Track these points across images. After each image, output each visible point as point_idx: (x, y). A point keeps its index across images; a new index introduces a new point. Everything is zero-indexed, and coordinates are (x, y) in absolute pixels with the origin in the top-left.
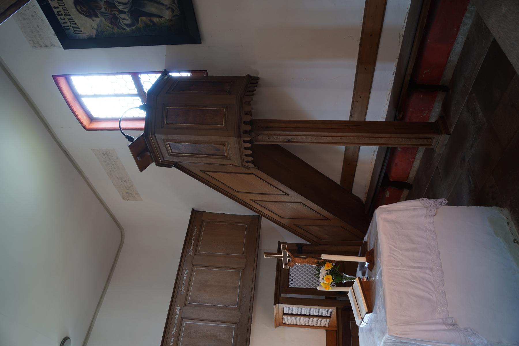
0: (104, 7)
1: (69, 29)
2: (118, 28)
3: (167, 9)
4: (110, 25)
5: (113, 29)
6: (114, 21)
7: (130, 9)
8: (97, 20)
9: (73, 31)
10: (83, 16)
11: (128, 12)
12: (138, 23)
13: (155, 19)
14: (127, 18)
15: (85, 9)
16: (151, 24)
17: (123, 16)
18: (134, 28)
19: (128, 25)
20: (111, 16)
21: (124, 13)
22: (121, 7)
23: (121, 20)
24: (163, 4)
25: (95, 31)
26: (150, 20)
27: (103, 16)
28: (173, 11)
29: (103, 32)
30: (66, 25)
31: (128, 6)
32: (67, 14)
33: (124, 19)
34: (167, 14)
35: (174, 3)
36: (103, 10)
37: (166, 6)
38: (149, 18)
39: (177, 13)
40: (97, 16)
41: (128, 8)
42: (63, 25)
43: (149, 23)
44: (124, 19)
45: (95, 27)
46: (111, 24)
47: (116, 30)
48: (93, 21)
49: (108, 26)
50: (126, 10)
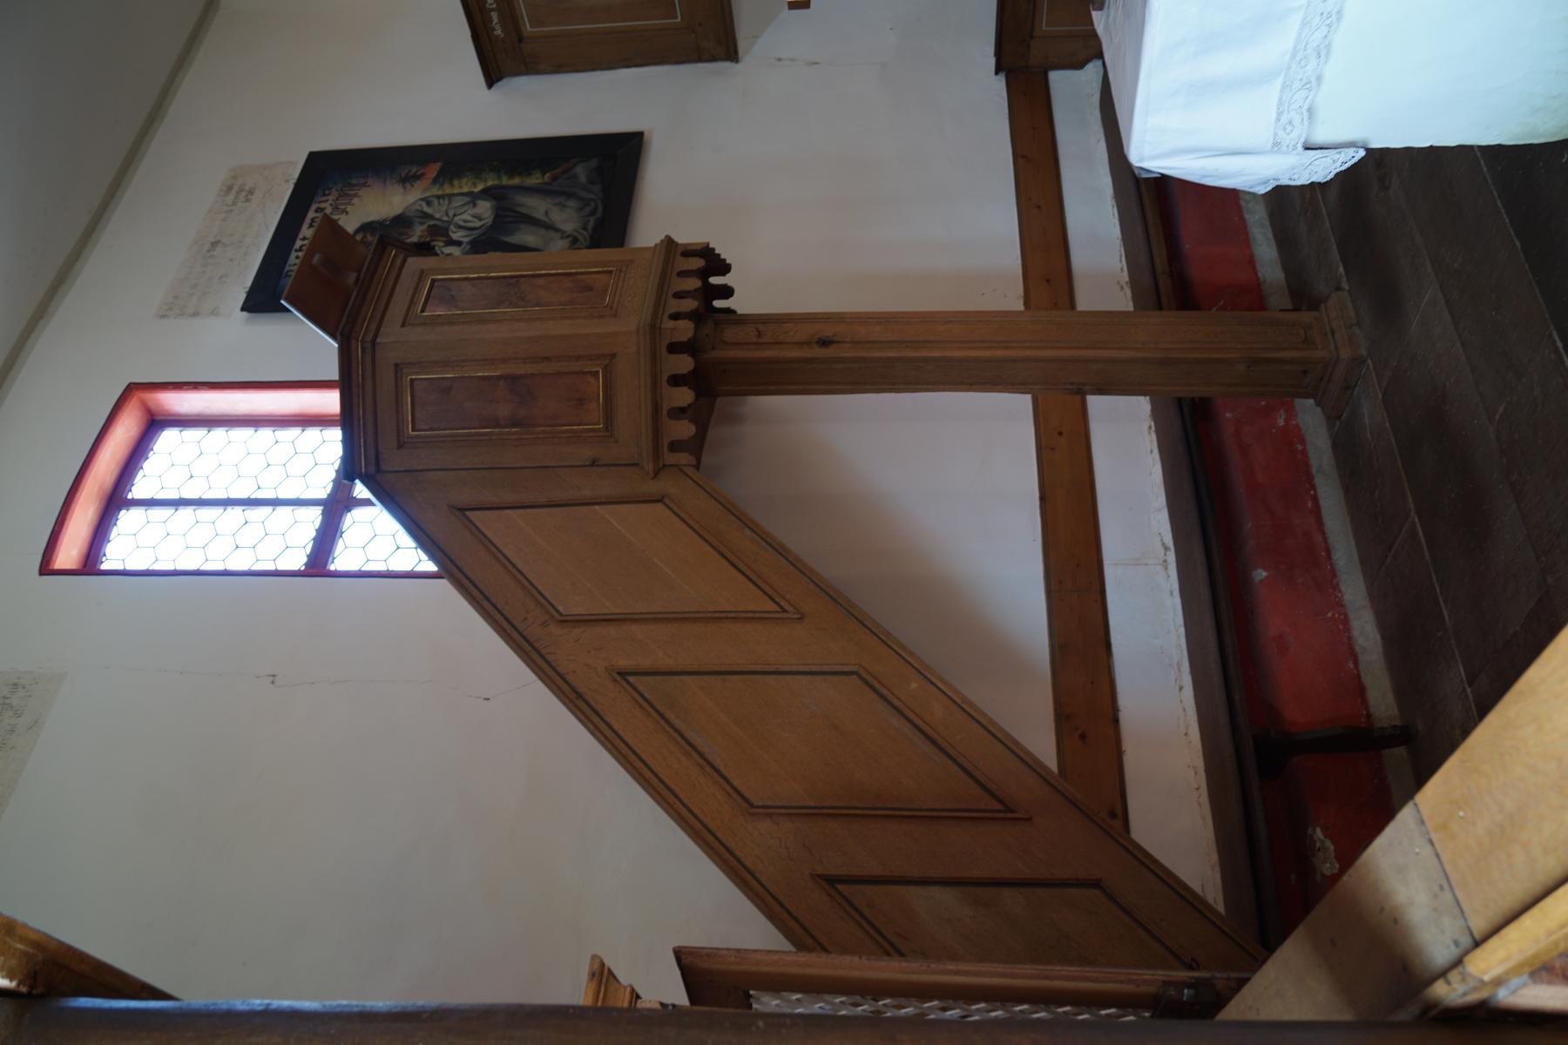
11: (470, 243)
21: (459, 244)
22: (456, 235)
24: (557, 230)
35: (585, 229)
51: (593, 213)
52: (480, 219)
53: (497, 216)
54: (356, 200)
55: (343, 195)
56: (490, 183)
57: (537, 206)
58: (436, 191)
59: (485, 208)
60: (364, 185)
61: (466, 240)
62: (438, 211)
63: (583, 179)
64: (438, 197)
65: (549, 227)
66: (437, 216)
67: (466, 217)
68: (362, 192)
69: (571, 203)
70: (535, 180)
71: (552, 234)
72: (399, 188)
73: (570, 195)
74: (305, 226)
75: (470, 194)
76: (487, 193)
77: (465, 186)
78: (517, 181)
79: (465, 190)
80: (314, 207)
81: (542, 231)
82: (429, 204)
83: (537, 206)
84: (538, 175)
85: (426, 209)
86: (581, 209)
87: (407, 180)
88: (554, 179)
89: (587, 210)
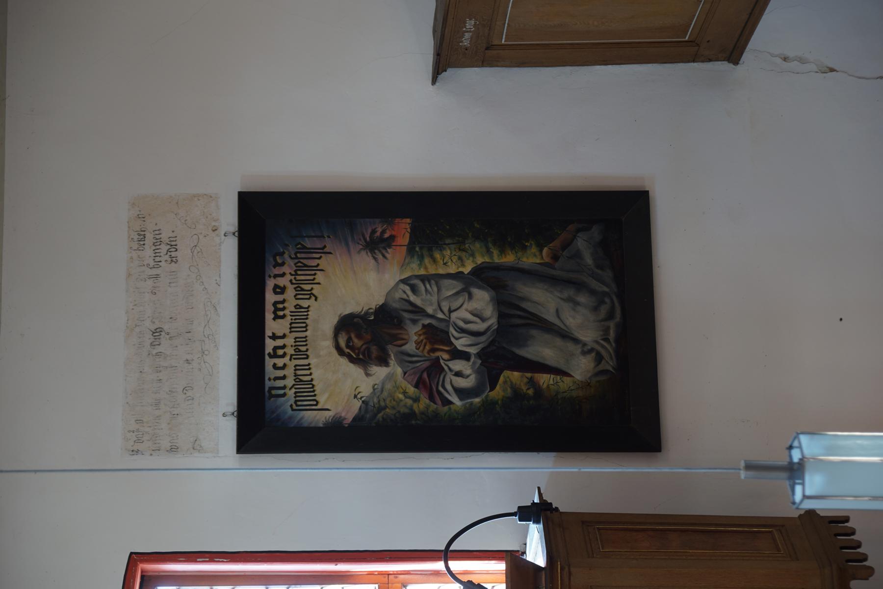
0: (415, 338)
1: (284, 395)
2: (431, 398)
3: (584, 353)
4: (411, 390)
5: (416, 400)
6: (429, 377)
7: (483, 349)
8: (380, 372)
9: (292, 401)
10: (344, 361)
11: (478, 355)
12: (492, 388)
13: (544, 379)
14: (468, 371)
15: (357, 342)
16: (531, 392)
17: (458, 365)
18: (477, 400)
19: (461, 393)
20: (427, 364)
22: (461, 343)
23: (450, 376)
24: (576, 341)
25: (357, 404)
26: (531, 382)
27: (401, 363)
28: (599, 358)
29: (381, 409)
30: (280, 383)
31: (483, 339)
32: (300, 353)
33: (458, 374)
34: (582, 368)
35: (606, 340)
36: (410, 347)
37: (585, 345)
38: (529, 375)
39: (609, 364)
40: (383, 361)
41: (481, 346)
42: (268, 384)
43: (524, 388)
44: (458, 374)
45: (366, 390)
46: (416, 386)
47: (425, 401)
48: (368, 375)
49: (404, 393)
50: (473, 350)
51: (610, 316)
52: (483, 320)
53: (501, 316)
54: (320, 277)
55: (301, 267)
56: (480, 260)
57: (543, 300)
58: (415, 269)
59: (482, 299)
60: (323, 251)
61: (473, 350)
62: (428, 300)
63: (589, 260)
64: (424, 279)
65: (566, 335)
66: (430, 311)
67: (463, 314)
68: (323, 263)
69: (582, 299)
70: (532, 258)
71: (571, 346)
72: (365, 260)
73: (579, 286)
74: (269, 316)
75: (458, 276)
76: (483, 276)
77: (450, 262)
78: (509, 258)
79: (452, 269)
80: (270, 284)
81: (559, 341)
82: (414, 289)
83: (543, 300)
84: (534, 249)
85: (412, 298)
86: (596, 309)
87: (377, 246)
88: (555, 258)
89: (604, 310)
